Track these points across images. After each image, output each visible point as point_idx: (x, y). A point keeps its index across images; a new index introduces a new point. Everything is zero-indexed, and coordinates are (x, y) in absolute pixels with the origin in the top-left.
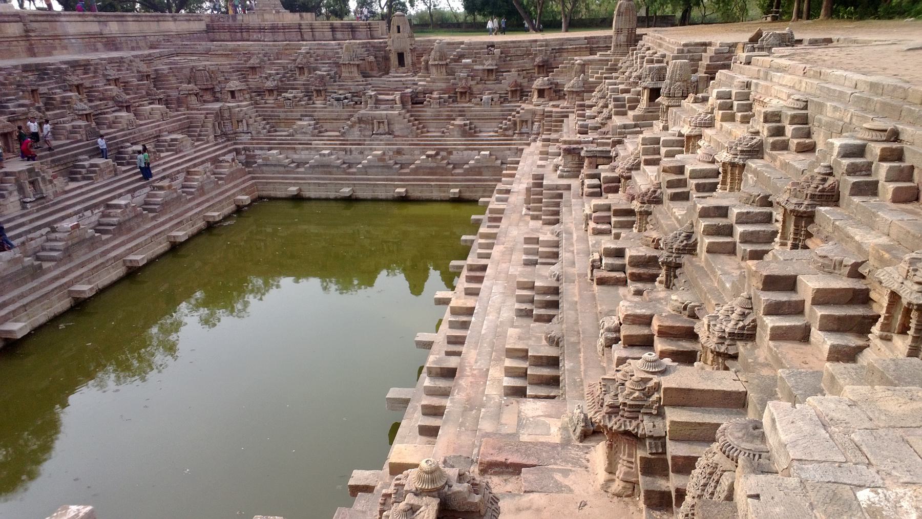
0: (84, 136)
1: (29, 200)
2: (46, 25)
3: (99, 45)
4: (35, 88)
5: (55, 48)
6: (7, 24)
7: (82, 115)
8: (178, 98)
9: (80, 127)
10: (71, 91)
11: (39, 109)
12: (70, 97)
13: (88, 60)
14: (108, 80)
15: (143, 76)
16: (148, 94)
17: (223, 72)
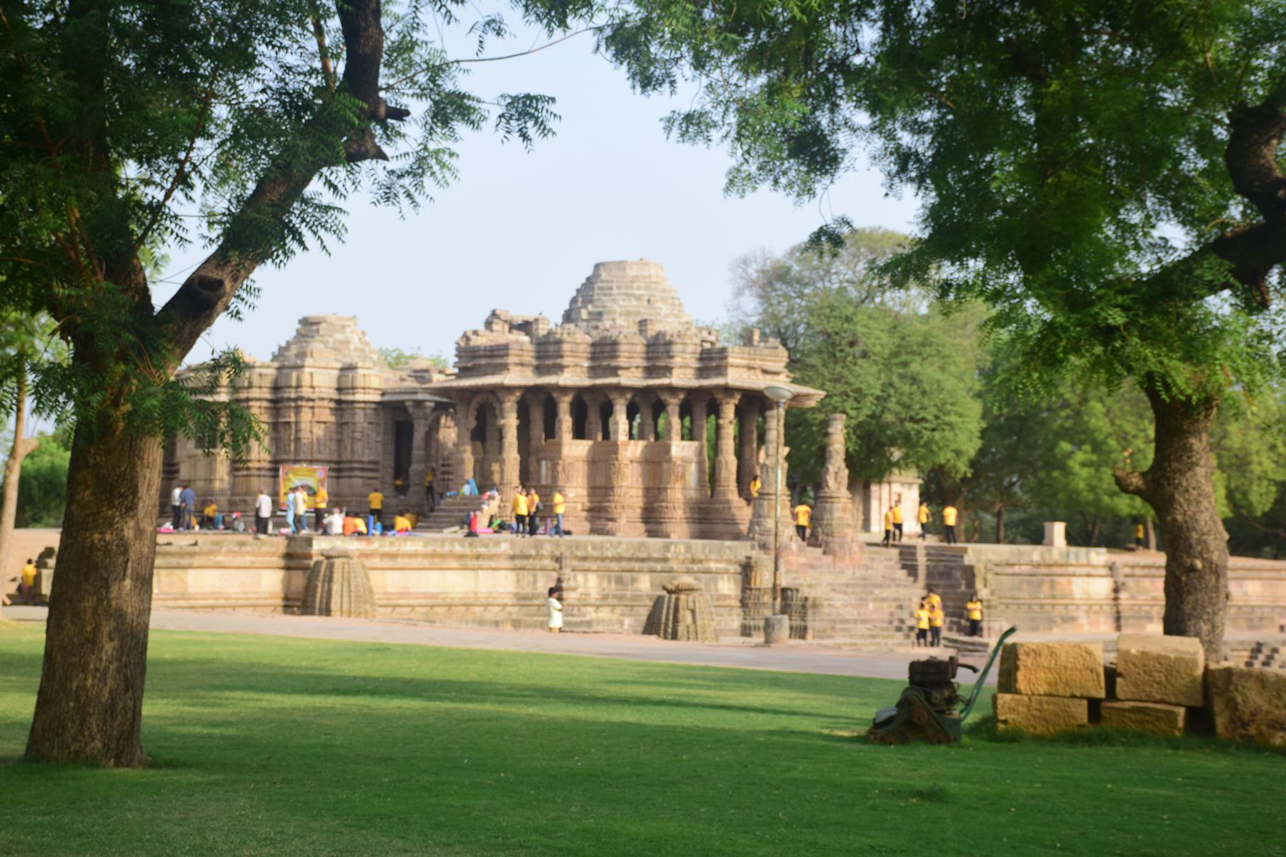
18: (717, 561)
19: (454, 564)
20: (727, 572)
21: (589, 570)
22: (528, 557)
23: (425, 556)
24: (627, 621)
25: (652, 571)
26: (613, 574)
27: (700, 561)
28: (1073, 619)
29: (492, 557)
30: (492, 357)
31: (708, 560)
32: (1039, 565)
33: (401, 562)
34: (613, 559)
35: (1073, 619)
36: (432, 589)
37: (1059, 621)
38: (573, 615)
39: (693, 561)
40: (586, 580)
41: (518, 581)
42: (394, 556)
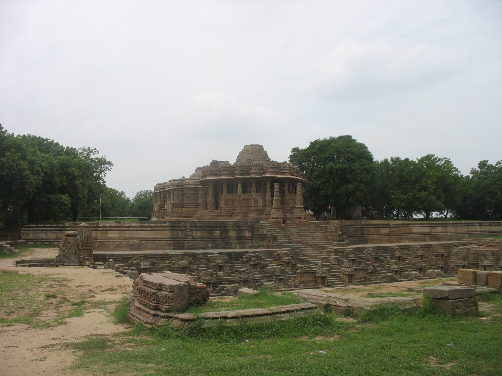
0: (388, 280)
3: (427, 238)
4: (377, 257)
5: (403, 239)
6: (382, 229)
7: (394, 271)
8: (453, 268)
9: (388, 275)
10: (395, 259)
11: (373, 266)
12: (391, 262)
13: (411, 246)
14: (418, 256)
15: (439, 254)
16: (436, 264)
17: (486, 255)
18: (244, 227)
20: (248, 230)
21: (197, 230)
22: (176, 227)
23: (139, 227)
26: (206, 231)
27: (239, 227)
30: (207, 172)
31: (242, 227)
33: (131, 229)
38: (189, 243)
40: (196, 233)
41: (171, 233)
42: (129, 227)
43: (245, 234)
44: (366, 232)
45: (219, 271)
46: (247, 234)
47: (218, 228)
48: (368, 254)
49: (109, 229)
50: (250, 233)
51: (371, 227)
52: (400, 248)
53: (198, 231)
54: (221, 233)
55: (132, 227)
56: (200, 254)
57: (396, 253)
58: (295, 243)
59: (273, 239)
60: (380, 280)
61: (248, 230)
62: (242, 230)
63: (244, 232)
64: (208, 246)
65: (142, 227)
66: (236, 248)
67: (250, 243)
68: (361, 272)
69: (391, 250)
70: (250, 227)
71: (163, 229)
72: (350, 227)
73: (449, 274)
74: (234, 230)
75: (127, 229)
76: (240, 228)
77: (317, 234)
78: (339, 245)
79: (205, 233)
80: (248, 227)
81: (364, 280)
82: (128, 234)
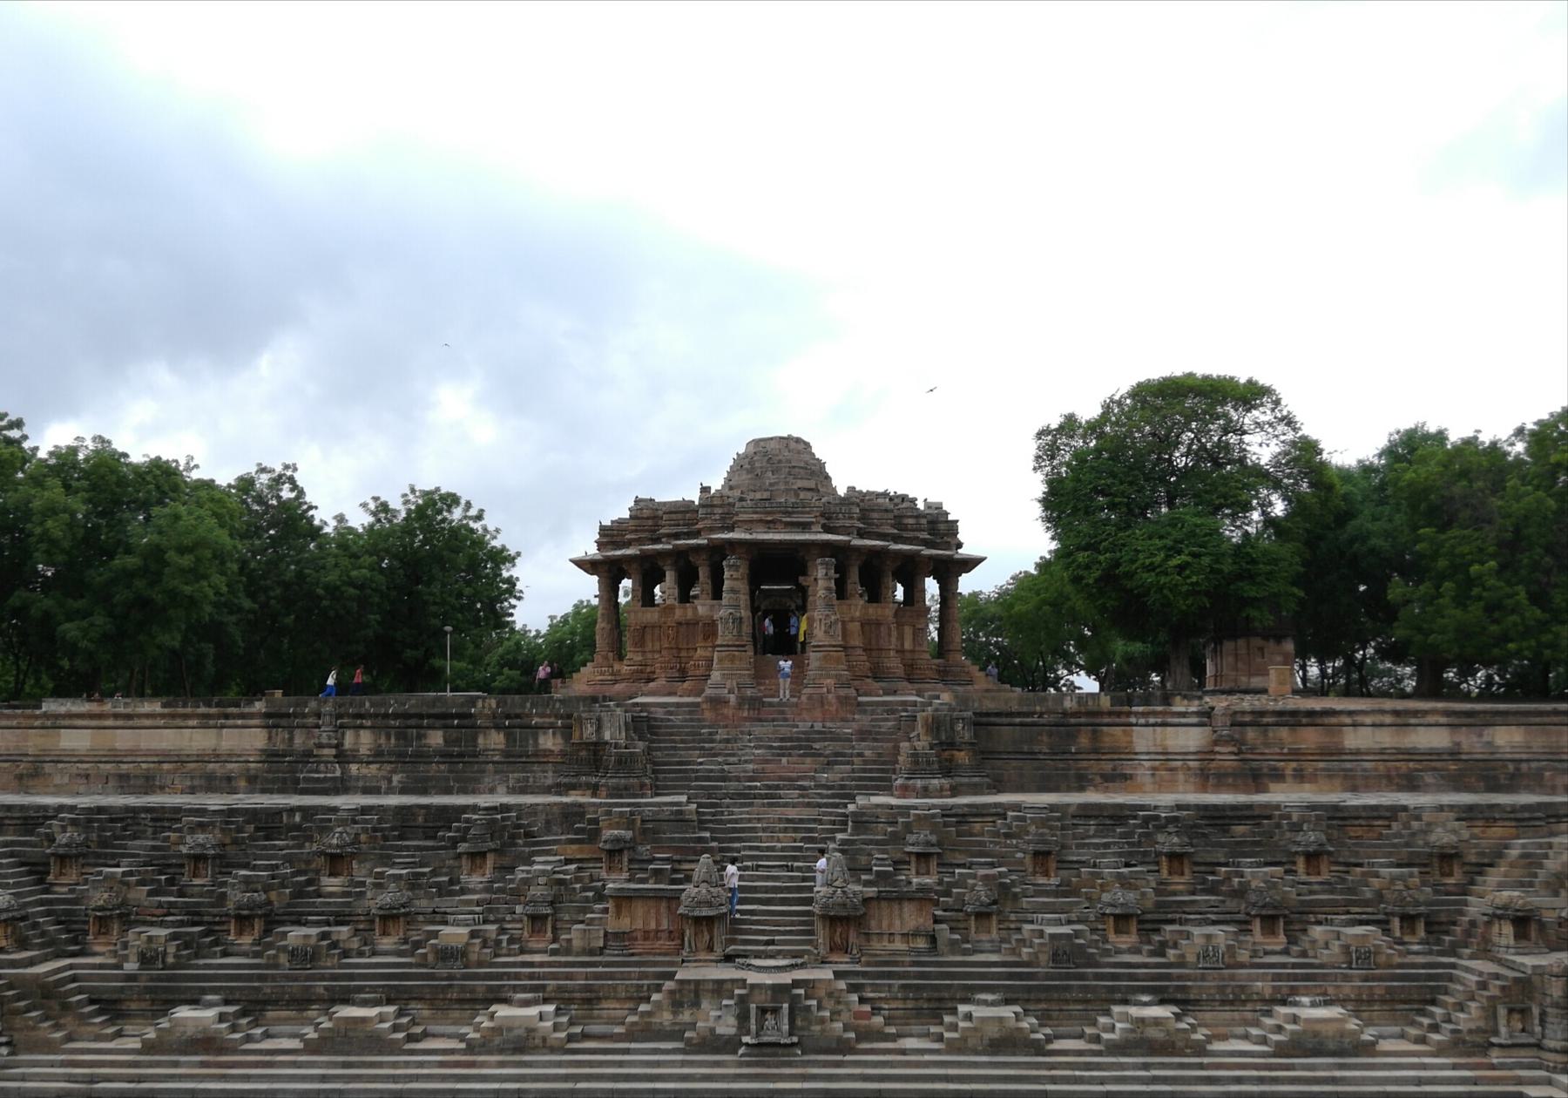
0: (1043, 958)
1: (746, 1039)
2: (1284, 733)
5: (1278, 776)
18: (542, 716)
19: (194, 722)
20: (552, 726)
21: (362, 727)
22: (288, 715)
23: (162, 716)
24: (396, 778)
25: (445, 727)
26: (393, 732)
27: (518, 716)
28: (1126, 777)
29: (243, 716)
32: (1076, 714)
33: (136, 722)
34: (396, 716)
35: (1126, 777)
36: (164, 745)
37: (1098, 780)
38: (317, 772)
39: (508, 717)
40: (358, 736)
41: (270, 738)
42: (129, 717)
43: (541, 740)
44: (1084, 741)
45: (331, 875)
46: (549, 742)
47: (439, 723)
48: (1007, 836)
49: (67, 722)
50: (559, 740)
51: (1106, 720)
52: (1202, 818)
53: (362, 732)
54: (445, 741)
55: (140, 716)
56: (292, 810)
57: (1161, 838)
58: (738, 779)
59: (619, 762)
60: (1013, 951)
61: (552, 726)
62: (530, 727)
63: (536, 740)
64: (390, 780)
65: (173, 716)
66: (492, 791)
67: (550, 774)
68: (908, 909)
69: (1147, 820)
70: (562, 717)
71: (239, 722)
72: (997, 720)
73: (1442, 953)
74: (498, 728)
75: (120, 723)
76: (525, 721)
77: (860, 746)
78: (905, 791)
79: (388, 738)
80: (557, 716)
81: (922, 944)
82: (123, 739)
